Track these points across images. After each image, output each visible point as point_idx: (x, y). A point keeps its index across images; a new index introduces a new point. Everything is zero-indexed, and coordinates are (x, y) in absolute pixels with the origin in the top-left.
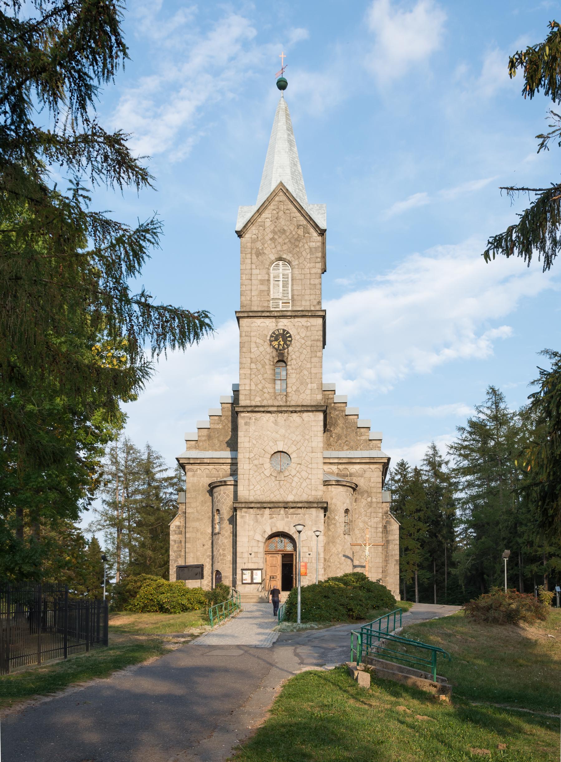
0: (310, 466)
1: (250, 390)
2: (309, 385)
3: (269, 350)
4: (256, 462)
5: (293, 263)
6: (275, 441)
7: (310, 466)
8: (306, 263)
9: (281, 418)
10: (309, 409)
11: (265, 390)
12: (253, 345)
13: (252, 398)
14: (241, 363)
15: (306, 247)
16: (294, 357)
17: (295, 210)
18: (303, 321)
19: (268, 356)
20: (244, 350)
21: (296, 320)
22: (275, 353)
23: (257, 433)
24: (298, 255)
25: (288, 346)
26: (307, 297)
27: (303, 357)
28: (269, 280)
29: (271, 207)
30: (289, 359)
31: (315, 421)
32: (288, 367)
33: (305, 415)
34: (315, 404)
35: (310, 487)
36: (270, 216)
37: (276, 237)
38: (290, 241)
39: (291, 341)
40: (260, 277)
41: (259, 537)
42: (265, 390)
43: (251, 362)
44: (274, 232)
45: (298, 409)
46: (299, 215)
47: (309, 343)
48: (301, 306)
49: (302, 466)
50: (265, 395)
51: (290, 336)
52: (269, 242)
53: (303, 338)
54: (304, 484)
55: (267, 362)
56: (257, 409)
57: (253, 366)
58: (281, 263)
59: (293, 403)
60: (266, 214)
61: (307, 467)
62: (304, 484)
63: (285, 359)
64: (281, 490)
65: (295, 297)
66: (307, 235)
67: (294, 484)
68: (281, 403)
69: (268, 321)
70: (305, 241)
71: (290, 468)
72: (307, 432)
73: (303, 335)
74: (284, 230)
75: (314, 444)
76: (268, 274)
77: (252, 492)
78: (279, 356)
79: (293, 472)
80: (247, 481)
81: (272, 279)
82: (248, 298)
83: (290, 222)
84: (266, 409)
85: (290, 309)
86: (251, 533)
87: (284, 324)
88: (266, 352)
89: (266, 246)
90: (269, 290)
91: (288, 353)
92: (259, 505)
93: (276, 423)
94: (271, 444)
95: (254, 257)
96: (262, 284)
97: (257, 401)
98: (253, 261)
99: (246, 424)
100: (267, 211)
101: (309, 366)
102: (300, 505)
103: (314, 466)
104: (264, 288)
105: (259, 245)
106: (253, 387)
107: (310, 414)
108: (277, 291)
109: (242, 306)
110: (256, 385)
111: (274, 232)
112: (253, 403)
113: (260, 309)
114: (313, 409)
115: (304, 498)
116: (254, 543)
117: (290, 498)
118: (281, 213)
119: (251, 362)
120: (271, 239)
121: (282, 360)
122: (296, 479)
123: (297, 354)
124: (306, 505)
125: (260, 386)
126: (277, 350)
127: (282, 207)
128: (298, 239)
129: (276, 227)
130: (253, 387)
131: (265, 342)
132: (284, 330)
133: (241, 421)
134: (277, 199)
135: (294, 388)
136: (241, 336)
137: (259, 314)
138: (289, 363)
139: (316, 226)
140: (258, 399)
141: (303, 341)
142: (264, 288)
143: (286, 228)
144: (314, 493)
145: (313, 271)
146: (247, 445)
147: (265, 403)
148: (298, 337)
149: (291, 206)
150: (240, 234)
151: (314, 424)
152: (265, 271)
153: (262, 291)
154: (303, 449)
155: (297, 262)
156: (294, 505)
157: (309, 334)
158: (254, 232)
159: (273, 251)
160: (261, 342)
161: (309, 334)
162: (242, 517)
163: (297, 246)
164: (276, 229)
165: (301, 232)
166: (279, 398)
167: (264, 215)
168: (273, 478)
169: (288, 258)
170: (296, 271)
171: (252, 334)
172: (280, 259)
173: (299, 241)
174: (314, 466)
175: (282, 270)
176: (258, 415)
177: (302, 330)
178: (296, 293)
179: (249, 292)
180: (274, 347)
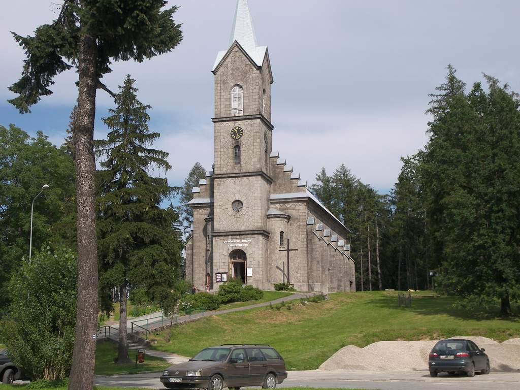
0: (254, 208)
1: (220, 164)
2: (253, 159)
3: (231, 139)
4: (224, 207)
5: (243, 87)
6: (234, 194)
7: (254, 208)
8: (250, 86)
9: (237, 180)
10: (253, 174)
11: (229, 164)
12: (222, 137)
13: (222, 169)
14: (215, 148)
15: (250, 77)
16: (244, 143)
17: (244, 56)
18: (249, 121)
19: (230, 143)
20: (217, 141)
21: (245, 121)
22: (234, 141)
23: (224, 190)
24: (246, 82)
25: (241, 136)
26: (251, 107)
27: (249, 142)
28: (230, 98)
29: (231, 55)
30: (242, 144)
31: (256, 180)
32: (241, 149)
33: (250, 178)
34: (256, 171)
35: (254, 221)
36: (230, 60)
37: (234, 73)
38: (242, 74)
39: (242, 134)
40: (225, 97)
41: (225, 253)
42: (229, 164)
43: (221, 148)
44: (233, 70)
45: (246, 174)
46: (246, 59)
47: (252, 134)
48: (248, 112)
49: (249, 209)
50: (229, 167)
51: (242, 131)
52: (230, 76)
53: (249, 131)
54: (251, 219)
55: (229, 147)
56: (223, 176)
57: (222, 150)
58: (237, 87)
59: (244, 171)
60: (229, 59)
61: (252, 209)
62: (251, 219)
63: (239, 144)
64: (238, 224)
65: (245, 107)
66: (251, 70)
67: (245, 220)
68: (238, 172)
69: (229, 123)
70: (250, 73)
71: (242, 210)
72: (252, 188)
73: (249, 130)
74: (238, 68)
75: (256, 195)
76: (230, 95)
77: (222, 226)
78: (236, 143)
79: (244, 213)
80: (219, 219)
81: (232, 97)
82: (219, 110)
83: (241, 63)
84: (229, 175)
85: (242, 114)
86: (221, 250)
87: (238, 123)
88: (228, 141)
89: (228, 78)
90: (230, 104)
91: (241, 141)
92: (225, 234)
93: (235, 183)
94: (232, 196)
95: (222, 85)
96: (226, 101)
97: (224, 171)
98: (222, 88)
99: (218, 185)
100: (229, 58)
101: (252, 148)
102: (247, 232)
103: (256, 208)
104: (228, 103)
105: (224, 78)
106: (222, 162)
107: (254, 177)
108: (235, 105)
109: (215, 115)
110: (224, 161)
111: (233, 70)
112: (222, 172)
113: (225, 116)
114: (255, 174)
115: (251, 228)
116: (223, 257)
117: (243, 228)
118: (237, 58)
119: (221, 148)
120: (231, 74)
121: (237, 147)
122: (246, 217)
123: (246, 141)
124: (251, 232)
125: (226, 161)
126: (235, 139)
127: (237, 54)
128: (246, 73)
129: (234, 66)
130: (222, 162)
131: (228, 135)
132: (239, 127)
133: (215, 184)
134: (234, 50)
135: (245, 161)
136: (215, 133)
137: (225, 119)
138: (241, 147)
139: (255, 65)
140: (225, 169)
141: (249, 133)
142: (228, 103)
143: (239, 67)
144: (256, 224)
145: (255, 91)
146: (219, 197)
147: (229, 172)
148: (246, 131)
149: (242, 54)
150: (214, 73)
151: (256, 182)
152: (228, 93)
153: (226, 105)
154: (249, 198)
155: (245, 87)
156: (244, 233)
157: (252, 128)
158: (222, 70)
159: (232, 80)
160: (226, 135)
161: (252, 128)
162: (216, 241)
163: (245, 77)
164: (234, 68)
165: (247, 68)
166: (236, 168)
167: (227, 60)
168: (233, 217)
169: (241, 84)
170: (245, 92)
171: (221, 131)
172: (237, 85)
173: (246, 74)
174: (256, 208)
175: (238, 91)
176: (225, 179)
177: (249, 126)
178: (245, 104)
179: (219, 106)
180: (233, 138)
